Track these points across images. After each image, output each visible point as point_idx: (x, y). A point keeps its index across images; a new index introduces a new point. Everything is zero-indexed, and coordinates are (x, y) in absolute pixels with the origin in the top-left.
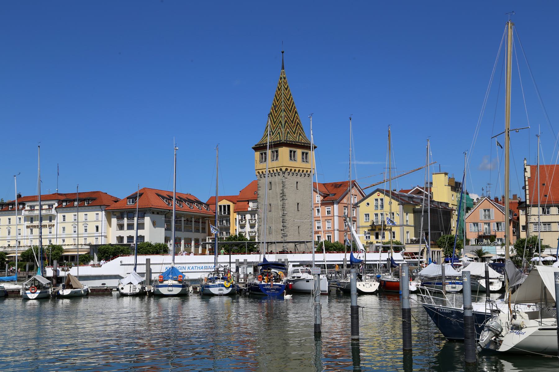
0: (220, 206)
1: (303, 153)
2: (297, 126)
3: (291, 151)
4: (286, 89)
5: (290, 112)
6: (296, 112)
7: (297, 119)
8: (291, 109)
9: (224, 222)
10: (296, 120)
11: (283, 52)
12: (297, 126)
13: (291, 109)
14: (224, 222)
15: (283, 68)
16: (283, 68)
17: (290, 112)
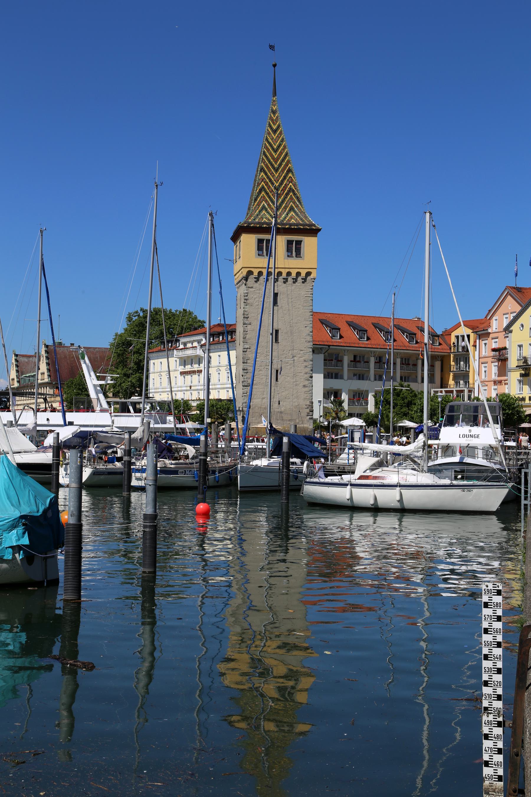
0: (457, 337)
1: (290, 243)
2: (287, 194)
3: (260, 241)
4: (275, 132)
5: (276, 170)
6: (289, 171)
7: (292, 181)
8: (280, 165)
9: (462, 363)
10: (286, 185)
11: (275, 66)
12: (287, 194)
13: (280, 165)
14: (462, 363)
15: (275, 94)
16: (275, 94)
17: (276, 170)
